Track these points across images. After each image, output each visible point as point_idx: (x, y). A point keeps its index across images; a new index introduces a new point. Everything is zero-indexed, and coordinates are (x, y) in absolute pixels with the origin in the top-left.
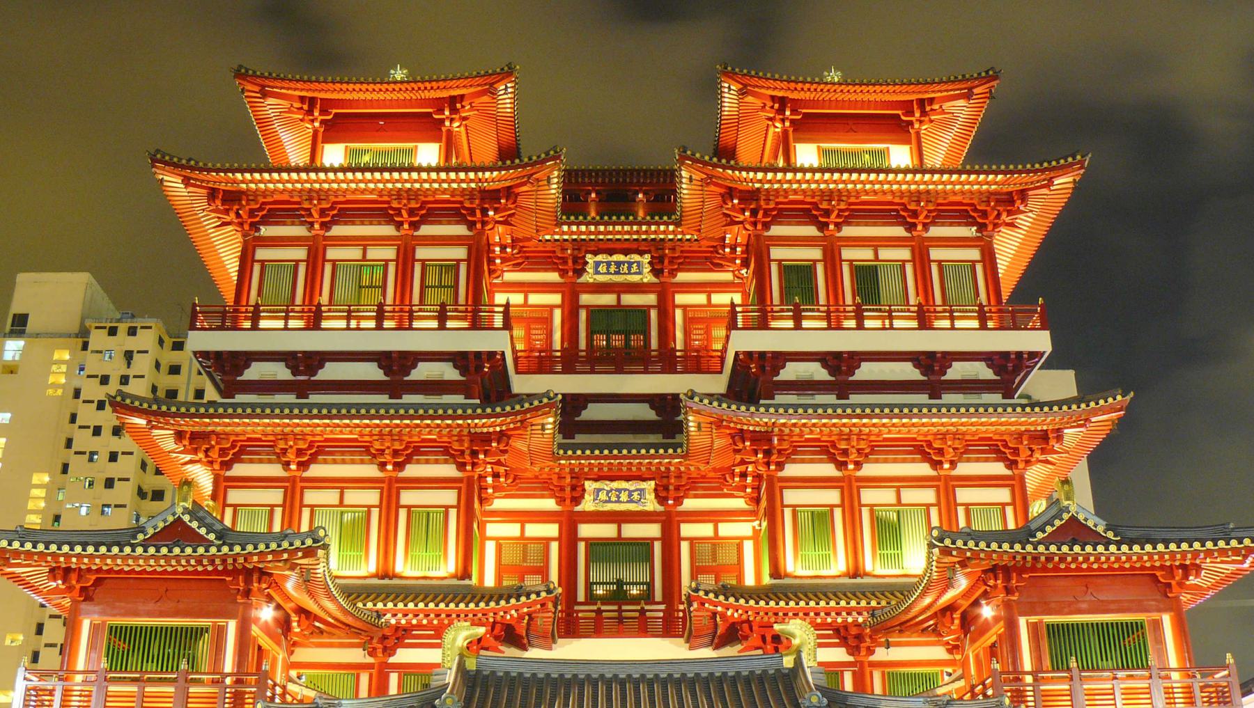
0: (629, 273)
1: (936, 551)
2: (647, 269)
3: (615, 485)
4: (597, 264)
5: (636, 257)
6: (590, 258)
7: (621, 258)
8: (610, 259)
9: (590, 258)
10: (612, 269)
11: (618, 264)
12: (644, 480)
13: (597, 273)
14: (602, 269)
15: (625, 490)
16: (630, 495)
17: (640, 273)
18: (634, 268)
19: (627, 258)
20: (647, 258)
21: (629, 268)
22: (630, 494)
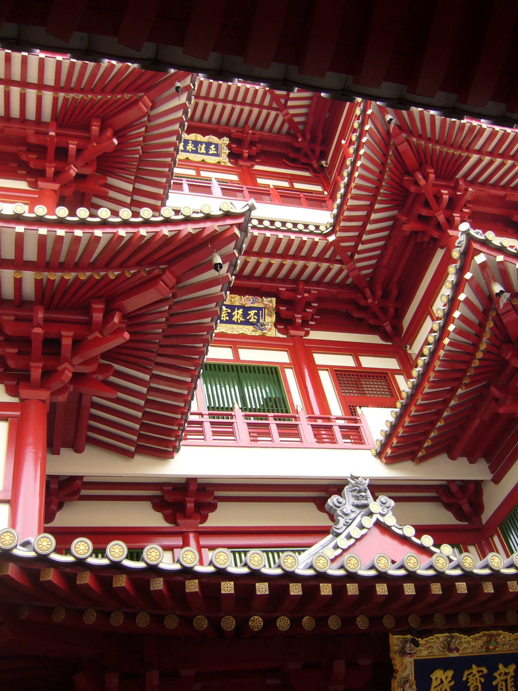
0: (207, 154)
5: (214, 139)
7: (199, 137)
10: (190, 147)
11: (196, 143)
15: (239, 307)
16: (245, 314)
17: (217, 155)
21: (207, 149)
22: (246, 310)
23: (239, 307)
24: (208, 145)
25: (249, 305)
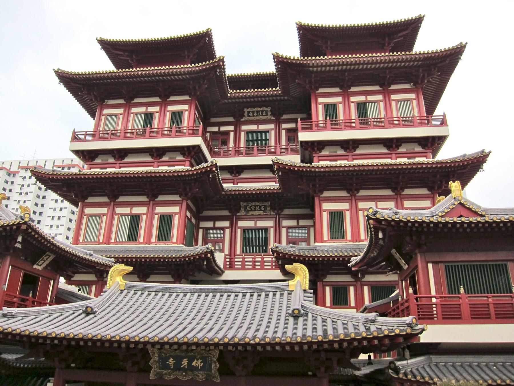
0: (262, 115)
1: (371, 221)
2: (269, 113)
3: (253, 204)
4: (249, 112)
5: (265, 109)
6: (246, 110)
7: (259, 109)
8: (254, 110)
9: (246, 110)
10: (255, 114)
11: (257, 112)
12: (266, 201)
13: (249, 116)
14: (251, 114)
15: (258, 206)
17: (267, 115)
18: (264, 114)
19: (261, 109)
20: (269, 109)
21: (262, 113)
22: (260, 207)
23: (258, 206)
24: (262, 111)
25: (261, 205)
